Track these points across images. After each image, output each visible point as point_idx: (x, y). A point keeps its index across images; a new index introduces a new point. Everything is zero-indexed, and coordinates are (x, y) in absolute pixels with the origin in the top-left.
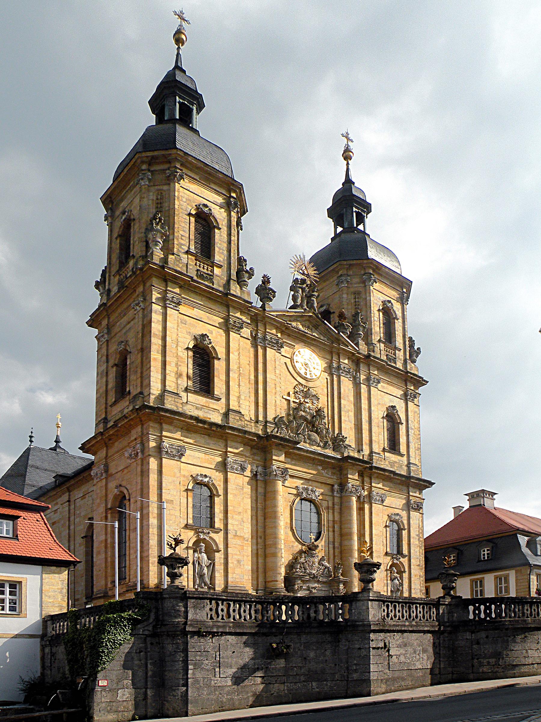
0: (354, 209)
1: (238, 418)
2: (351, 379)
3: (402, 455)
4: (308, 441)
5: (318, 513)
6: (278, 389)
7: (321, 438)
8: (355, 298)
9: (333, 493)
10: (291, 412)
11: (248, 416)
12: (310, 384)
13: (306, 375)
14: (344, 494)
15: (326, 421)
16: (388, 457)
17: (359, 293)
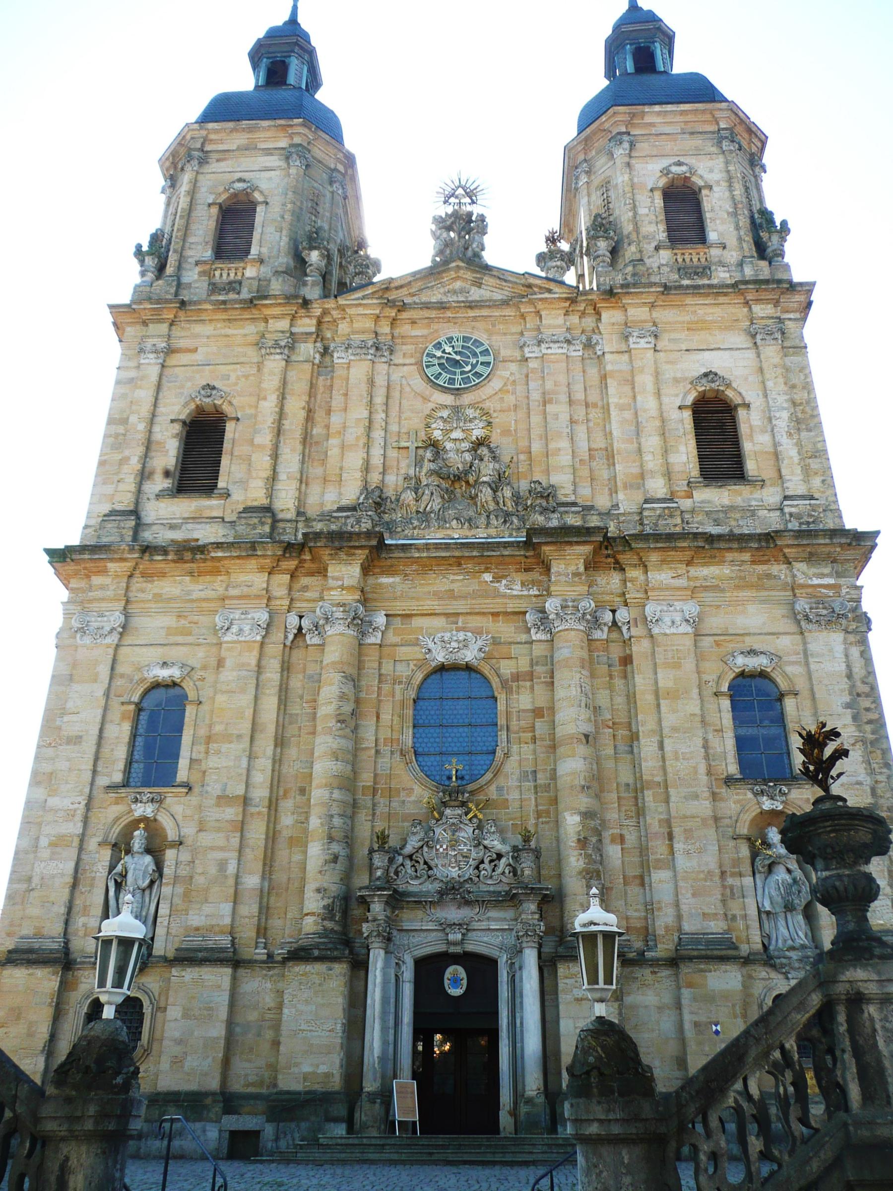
1: (256, 521)
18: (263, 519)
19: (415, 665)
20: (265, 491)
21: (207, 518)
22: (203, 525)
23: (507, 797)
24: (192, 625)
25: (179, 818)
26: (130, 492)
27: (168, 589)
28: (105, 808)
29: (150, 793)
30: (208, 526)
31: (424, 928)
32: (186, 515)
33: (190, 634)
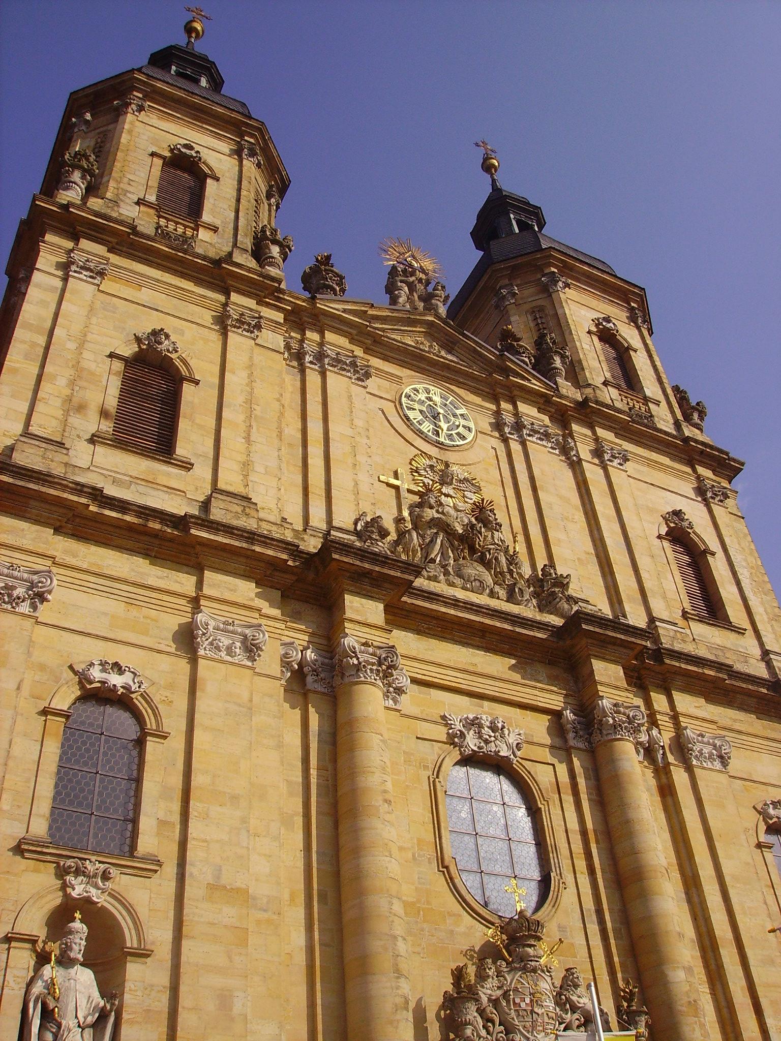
0: (512, 216)
1: (239, 509)
2: (557, 452)
4: (458, 581)
5: (534, 812)
6: (362, 459)
7: (499, 576)
8: (536, 319)
9: (566, 741)
10: (406, 513)
11: (276, 512)
12: (451, 457)
13: (438, 434)
14: (596, 737)
15: (505, 535)
16: (699, 635)
17: (541, 309)
18: (247, 510)
19: (440, 748)
20: (241, 477)
21: (165, 486)
22: (160, 493)
23: (573, 941)
24: (149, 621)
25: (143, 913)
27: (111, 562)
29: (100, 862)
30: (166, 496)
32: (134, 474)
33: (145, 633)
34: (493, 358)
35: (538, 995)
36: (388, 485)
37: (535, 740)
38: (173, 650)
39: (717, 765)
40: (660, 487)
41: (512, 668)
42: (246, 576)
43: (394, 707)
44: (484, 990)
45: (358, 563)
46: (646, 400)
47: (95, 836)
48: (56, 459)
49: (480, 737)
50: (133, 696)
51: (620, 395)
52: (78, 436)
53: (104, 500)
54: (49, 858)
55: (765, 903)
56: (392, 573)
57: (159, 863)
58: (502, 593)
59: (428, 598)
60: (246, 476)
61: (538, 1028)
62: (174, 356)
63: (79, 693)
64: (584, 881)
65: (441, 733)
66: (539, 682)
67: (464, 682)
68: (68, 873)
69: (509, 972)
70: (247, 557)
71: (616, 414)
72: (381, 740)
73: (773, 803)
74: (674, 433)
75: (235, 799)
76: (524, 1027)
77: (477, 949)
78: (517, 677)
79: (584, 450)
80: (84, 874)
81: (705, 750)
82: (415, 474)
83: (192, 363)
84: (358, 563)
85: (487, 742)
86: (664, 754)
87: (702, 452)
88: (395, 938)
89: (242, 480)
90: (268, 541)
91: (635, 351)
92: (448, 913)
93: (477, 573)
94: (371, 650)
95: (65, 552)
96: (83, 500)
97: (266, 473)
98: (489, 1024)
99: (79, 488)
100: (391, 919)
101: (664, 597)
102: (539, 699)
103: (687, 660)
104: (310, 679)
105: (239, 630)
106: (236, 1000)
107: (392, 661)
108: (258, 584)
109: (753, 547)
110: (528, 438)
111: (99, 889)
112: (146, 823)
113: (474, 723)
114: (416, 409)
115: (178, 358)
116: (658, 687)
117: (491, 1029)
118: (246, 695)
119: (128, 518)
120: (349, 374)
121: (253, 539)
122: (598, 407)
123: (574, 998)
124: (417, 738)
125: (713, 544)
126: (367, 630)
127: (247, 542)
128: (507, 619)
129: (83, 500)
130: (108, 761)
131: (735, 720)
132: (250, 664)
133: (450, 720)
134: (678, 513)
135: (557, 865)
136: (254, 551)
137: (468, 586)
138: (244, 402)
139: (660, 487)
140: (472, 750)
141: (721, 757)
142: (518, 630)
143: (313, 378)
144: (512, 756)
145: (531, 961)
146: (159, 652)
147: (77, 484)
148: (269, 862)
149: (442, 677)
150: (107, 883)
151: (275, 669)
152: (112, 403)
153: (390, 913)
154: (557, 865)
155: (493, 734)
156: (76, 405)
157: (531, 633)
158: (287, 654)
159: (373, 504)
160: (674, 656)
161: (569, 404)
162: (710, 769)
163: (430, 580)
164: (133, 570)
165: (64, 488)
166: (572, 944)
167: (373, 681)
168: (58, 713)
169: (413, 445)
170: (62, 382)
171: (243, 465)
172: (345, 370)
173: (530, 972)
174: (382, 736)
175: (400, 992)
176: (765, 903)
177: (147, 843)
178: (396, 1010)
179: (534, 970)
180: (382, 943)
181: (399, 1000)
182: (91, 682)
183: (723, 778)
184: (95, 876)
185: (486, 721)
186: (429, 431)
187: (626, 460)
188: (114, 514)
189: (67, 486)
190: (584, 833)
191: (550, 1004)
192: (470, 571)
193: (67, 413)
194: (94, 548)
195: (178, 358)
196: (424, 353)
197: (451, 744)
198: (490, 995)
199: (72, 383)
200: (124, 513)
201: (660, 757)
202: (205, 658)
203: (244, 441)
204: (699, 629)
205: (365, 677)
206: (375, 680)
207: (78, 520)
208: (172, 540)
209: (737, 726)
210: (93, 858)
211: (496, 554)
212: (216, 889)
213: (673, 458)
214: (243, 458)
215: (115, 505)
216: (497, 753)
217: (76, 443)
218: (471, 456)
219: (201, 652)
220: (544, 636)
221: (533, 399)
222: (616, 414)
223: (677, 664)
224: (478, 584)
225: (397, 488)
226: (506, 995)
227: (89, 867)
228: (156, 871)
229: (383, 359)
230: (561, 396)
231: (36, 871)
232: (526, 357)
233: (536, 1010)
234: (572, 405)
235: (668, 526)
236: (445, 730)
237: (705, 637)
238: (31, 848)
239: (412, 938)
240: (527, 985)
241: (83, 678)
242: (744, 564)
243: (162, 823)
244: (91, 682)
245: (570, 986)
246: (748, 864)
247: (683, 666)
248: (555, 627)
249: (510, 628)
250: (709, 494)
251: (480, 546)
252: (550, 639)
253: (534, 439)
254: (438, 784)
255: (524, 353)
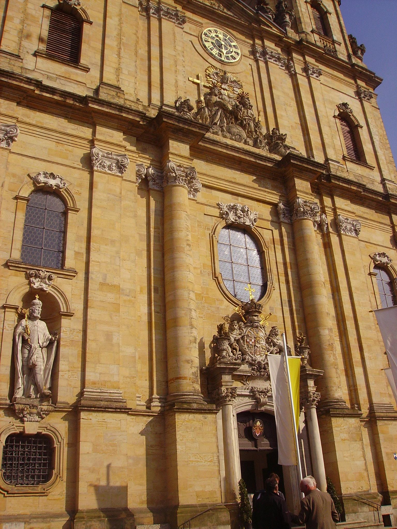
1: (114, 93)
2: (284, 68)
3: (371, 168)
4: (228, 135)
5: (261, 253)
6: (180, 68)
7: (250, 133)
9: (279, 218)
10: (202, 98)
11: (134, 95)
12: (227, 69)
13: (221, 56)
14: (294, 218)
15: (254, 112)
16: (350, 169)
18: (119, 94)
19: (216, 220)
20: (115, 76)
21: (75, 81)
22: (72, 84)
23: (276, 314)
25: (69, 296)
26: (15, 42)
27: (47, 121)
28: (6, 277)
29: (47, 272)
30: (76, 86)
31: (243, 393)
32: (59, 74)
33: (67, 158)
34: (253, 15)
35: (258, 338)
36: (194, 82)
37: (264, 218)
38: (81, 167)
39: (354, 234)
40: (337, 90)
41: (254, 181)
42: (118, 129)
43: (193, 198)
44: (232, 335)
45: (176, 124)
46: (334, 42)
47: (44, 259)
48: (16, 65)
49: (236, 215)
50: (61, 190)
51: (320, 38)
52: (28, 52)
53: (43, 87)
54: (22, 269)
55: (370, 301)
56: (194, 129)
57: (76, 272)
58: (251, 142)
59: (212, 143)
60: (118, 76)
61: (257, 353)
62: (78, 7)
63: (33, 188)
64: (284, 286)
65: (216, 212)
66: (267, 188)
67: (230, 187)
68: (32, 277)
69: (245, 327)
70: (118, 119)
71: (317, 49)
72: (186, 215)
73: (379, 254)
74: (347, 61)
75: (113, 242)
76: (251, 352)
77: (230, 316)
78: (256, 186)
79: (298, 68)
80: (39, 277)
81: (348, 227)
82: (208, 77)
83: (88, 12)
84: (176, 124)
85: (239, 218)
86: (327, 227)
87: (361, 72)
88: (191, 310)
89: (116, 78)
90: (130, 111)
91: (330, 14)
92: (217, 299)
93: (238, 131)
94: (182, 169)
95: (23, 115)
96: (32, 88)
97: (129, 74)
98: (234, 351)
99: (29, 80)
100: (189, 301)
101: (334, 148)
102: (267, 197)
103: (343, 181)
104: (151, 183)
105: (115, 157)
106: (114, 336)
107: (193, 175)
108: (124, 134)
109: (382, 124)
110: (269, 60)
111: (46, 284)
112: (69, 253)
113: (233, 208)
114: (209, 42)
115: (81, 9)
116: (327, 194)
117: (235, 353)
118: (118, 190)
119: (55, 97)
120: (174, 21)
121: (122, 110)
122: (308, 45)
123: (275, 340)
124: (205, 214)
125: (362, 122)
126: (181, 159)
127: (118, 111)
128: (252, 156)
129: (32, 88)
130: (49, 223)
131: (364, 213)
132: (120, 175)
133: (221, 206)
134: (345, 105)
135: (271, 279)
136: (122, 116)
137: (234, 138)
138: (117, 35)
139: (337, 90)
140: (232, 221)
141: (356, 230)
142: (258, 161)
143: (154, 23)
144: (252, 225)
145: (256, 323)
146: (74, 168)
147: (28, 78)
148: (130, 272)
149: (218, 184)
150: (50, 282)
151: (133, 177)
152: (45, 34)
153: (189, 298)
154: (271, 279)
155: (242, 214)
156: (25, 34)
157: (265, 164)
158: (139, 170)
159: (185, 93)
160: (337, 179)
161: (292, 42)
162: (350, 236)
163: (214, 134)
164: (59, 125)
165: (21, 81)
166: (276, 316)
167: (183, 185)
168: (23, 199)
169: (207, 61)
170: (17, 21)
171: (117, 70)
172: (172, 18)
173: (255, 328)
174: (187, 212)
175: (192, 335)
176: (370, 301)
177: (70, 262)
178: (190, 343)
179: (257, 327)
180: (185, 312)
181: (192, 339)
182: (39, 183)
183: (356, 241)
184: (45, 278)
185: (239, 207)
186: (216, 54)
187: (320, 74)
188: (48, 95)
189: (23, 80)
190: (285, 264)
191: (263, 343)
192: (235, 130)
193: (20, 39)
194: (38, 113)
195: (81, 9)
196: (215, 10)
197: (221, 218)
198: (235, 338)
199: (23, 22)
200: (53, 95)
201: (325, 228)
202: (97, 171)
203: (116, 56)
204: (350, 166)
205: (179, 183)
206: (184, 184)
207: (29, 98)
208: (79, 109)
209: (365, 216)
210: (44, 270)
211: (249, 122)
212: (103, 285)
213: (345, 74)
214: (116, 66)
215: (49, 90)
216: (244, 223)
217: (26, 56)
218: (238, 68)
219: (95, 168)
220: (271, 166)
221: (273, 38)
222: (317, 49)
223: (338, 183)
224: (238, 137)
225: (198, 84)
226: (243, 338)
227: (42, 274)
228: (74, 276)
229: (193, 13)
230: (288, 38)
231: (16, 275)
232: (270, 14)
233: (257, 345)
234: (293, 43)
235: (339, 111)
236: (218, 211)
237: (353, 170)
238: (13, 265)
239: (199, 310)
240: (253, 334)
241: (35, 181)
242: (377, 133)
243: (77, 253)
244: (39, 183)
245: (274, 335)
246: (363, 282)
247: (341, 184)
248: (277, 161)
249: (254, 160)
250: (362, 95)
251: (240, 117)
252: (274, 167)
253: (272, 61)
254: (214, 237)
255: (269, 12)
